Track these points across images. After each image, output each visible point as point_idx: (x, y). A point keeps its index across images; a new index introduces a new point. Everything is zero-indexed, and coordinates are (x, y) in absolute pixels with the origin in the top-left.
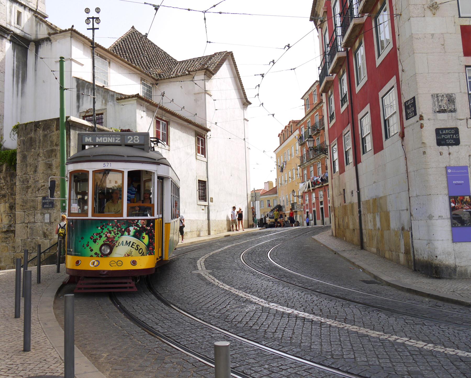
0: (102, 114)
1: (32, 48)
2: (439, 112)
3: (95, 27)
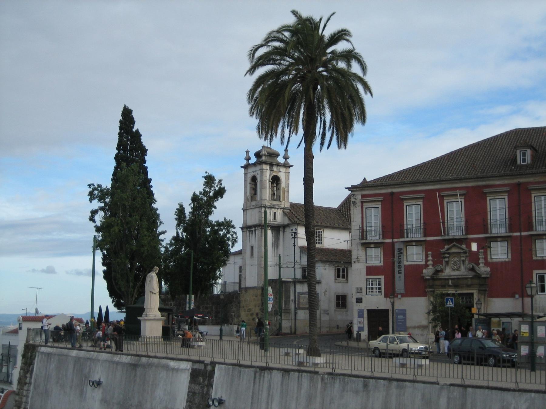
1: (282, 229)
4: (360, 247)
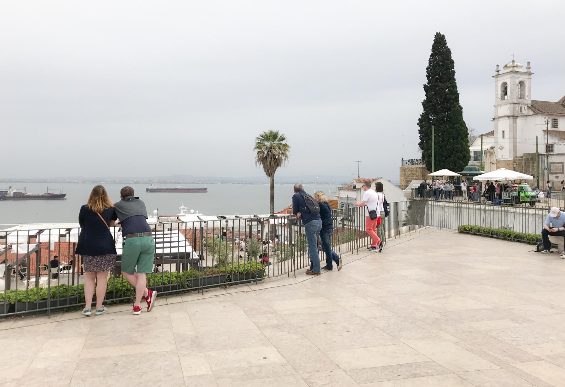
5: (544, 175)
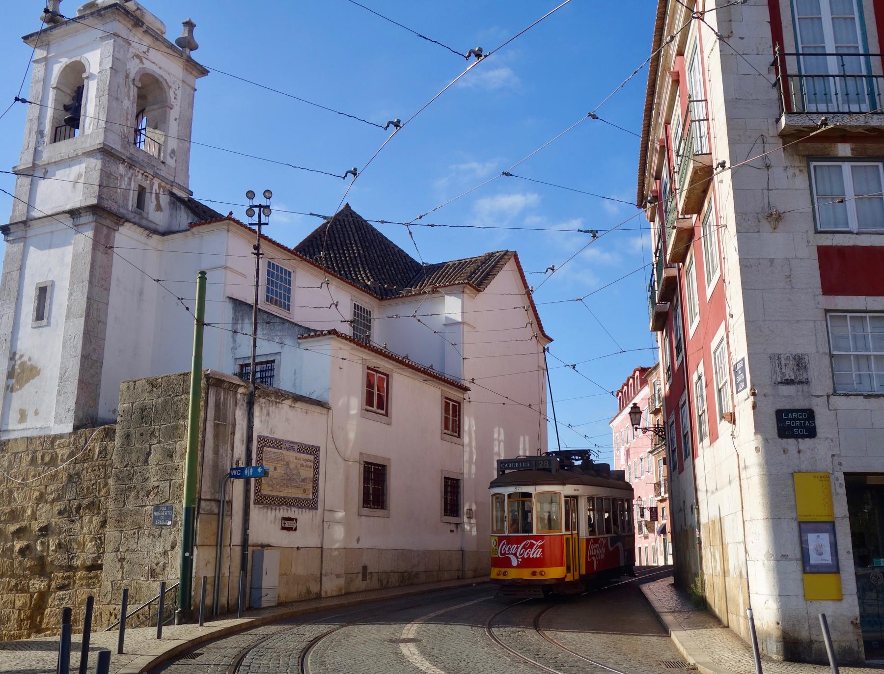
0: (273, 362)
2: (781, 383)
3: (263, 221)
4: (775, 150)
5: (223, 506)
